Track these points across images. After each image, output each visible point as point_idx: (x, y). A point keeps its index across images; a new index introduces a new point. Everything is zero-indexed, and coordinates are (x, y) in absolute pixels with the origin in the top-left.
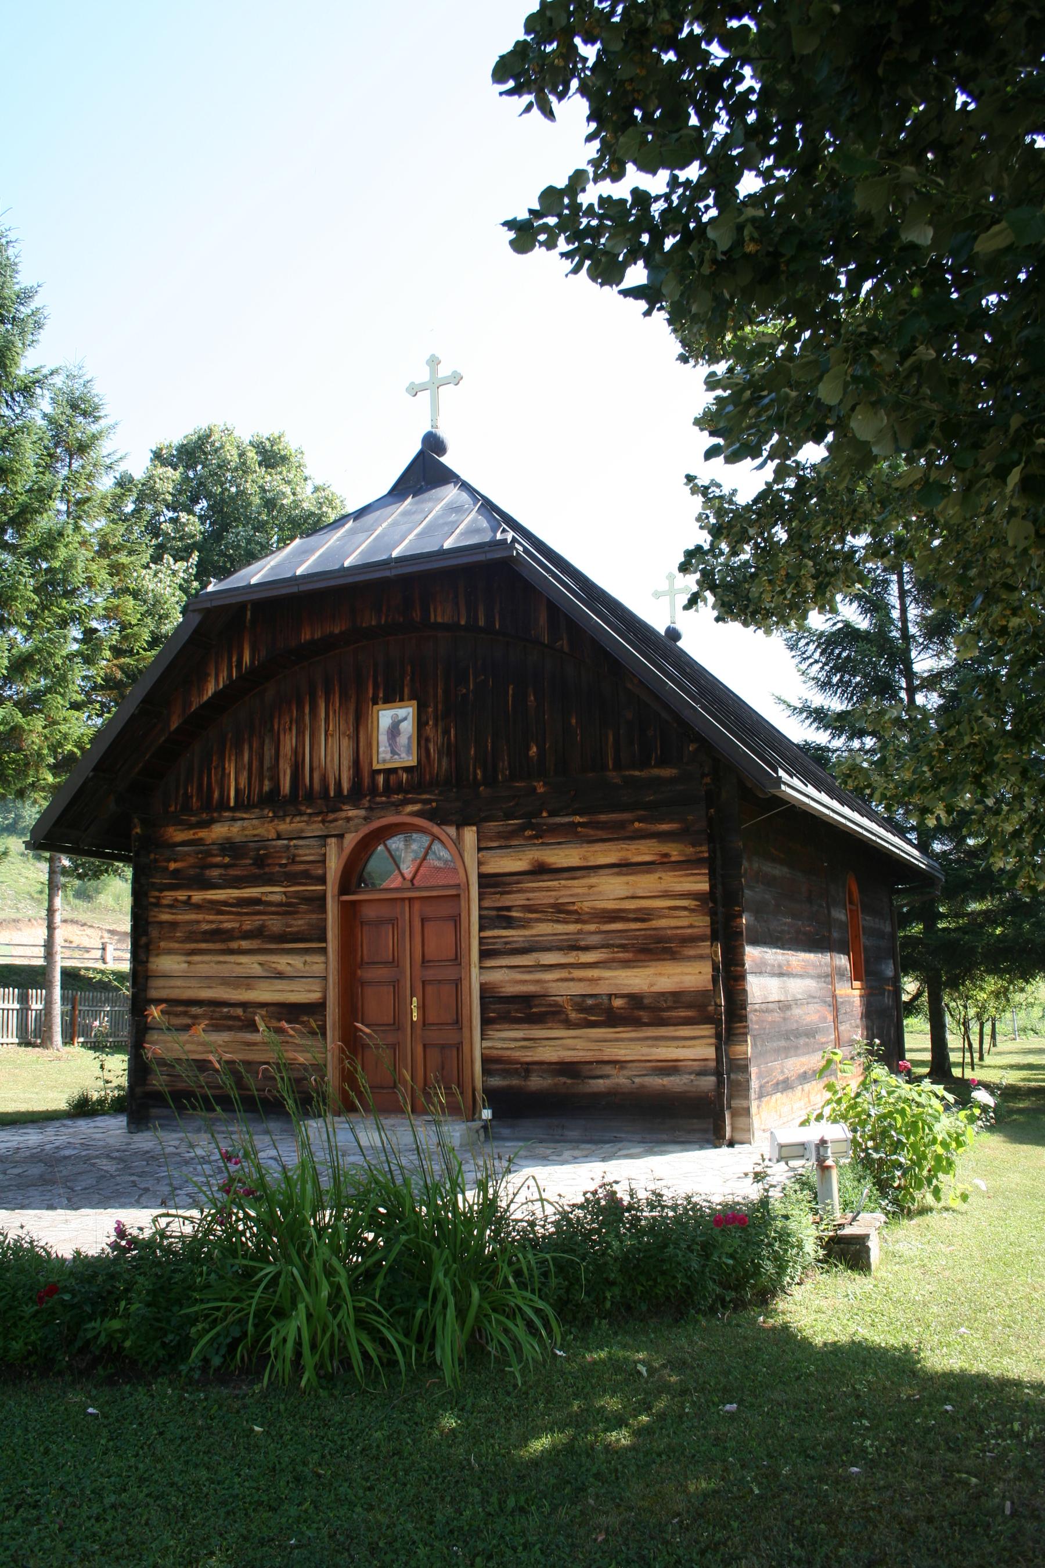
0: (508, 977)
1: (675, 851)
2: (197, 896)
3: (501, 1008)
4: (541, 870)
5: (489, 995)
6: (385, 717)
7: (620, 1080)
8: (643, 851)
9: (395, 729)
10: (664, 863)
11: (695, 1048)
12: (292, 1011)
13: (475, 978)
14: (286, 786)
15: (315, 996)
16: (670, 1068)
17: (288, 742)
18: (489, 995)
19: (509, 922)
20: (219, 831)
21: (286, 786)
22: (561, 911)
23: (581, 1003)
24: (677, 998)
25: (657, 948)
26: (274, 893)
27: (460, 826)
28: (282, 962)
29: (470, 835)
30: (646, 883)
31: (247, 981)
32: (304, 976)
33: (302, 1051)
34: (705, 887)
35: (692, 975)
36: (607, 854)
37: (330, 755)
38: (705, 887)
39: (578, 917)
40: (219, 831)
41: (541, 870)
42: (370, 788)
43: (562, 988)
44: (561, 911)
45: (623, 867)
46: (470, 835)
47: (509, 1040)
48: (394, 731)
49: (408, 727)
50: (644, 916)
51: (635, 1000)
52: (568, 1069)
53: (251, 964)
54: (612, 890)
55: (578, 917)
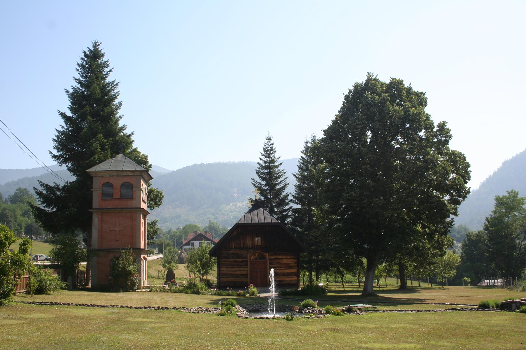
1: (292, 257)
2: (228, 260)
4: (276, 258)
6: (256, 239)
7: (286, 282)
8: (289, 257)
10: (291, 258)
11: (295, 278)
14: (242, 246)
15: (246, 273)
16: (292, 281)
17: (242, 241)
19: (273, 264)
20: (231, 252)
21: (242, 246)
22: (279, 263)
23: (281, 273)
24: (293, 273)
25: (290, 268)
26: (240, 260)
27: (266, 252)
28: (241, 269)
29: (267, 254)
30: (289, 260)
31: (236, 271)
32: (244, 271)
34: (296, 261)
35: (294, 271)
36: (285, 257)
37: (249, 243)
38: (296, 261)
39: (281, 264)
40: (231, 252)
41: (276, 258)
42: (254, 248)
44: (279, 263)
45: (286, 258)
46: (267, 254)
48: (258, 241)
49: (260, 240)
50: (289, 264)
51: (288, 273)
53: (237, 269)
54: (285, 261)
55: (281, 264)
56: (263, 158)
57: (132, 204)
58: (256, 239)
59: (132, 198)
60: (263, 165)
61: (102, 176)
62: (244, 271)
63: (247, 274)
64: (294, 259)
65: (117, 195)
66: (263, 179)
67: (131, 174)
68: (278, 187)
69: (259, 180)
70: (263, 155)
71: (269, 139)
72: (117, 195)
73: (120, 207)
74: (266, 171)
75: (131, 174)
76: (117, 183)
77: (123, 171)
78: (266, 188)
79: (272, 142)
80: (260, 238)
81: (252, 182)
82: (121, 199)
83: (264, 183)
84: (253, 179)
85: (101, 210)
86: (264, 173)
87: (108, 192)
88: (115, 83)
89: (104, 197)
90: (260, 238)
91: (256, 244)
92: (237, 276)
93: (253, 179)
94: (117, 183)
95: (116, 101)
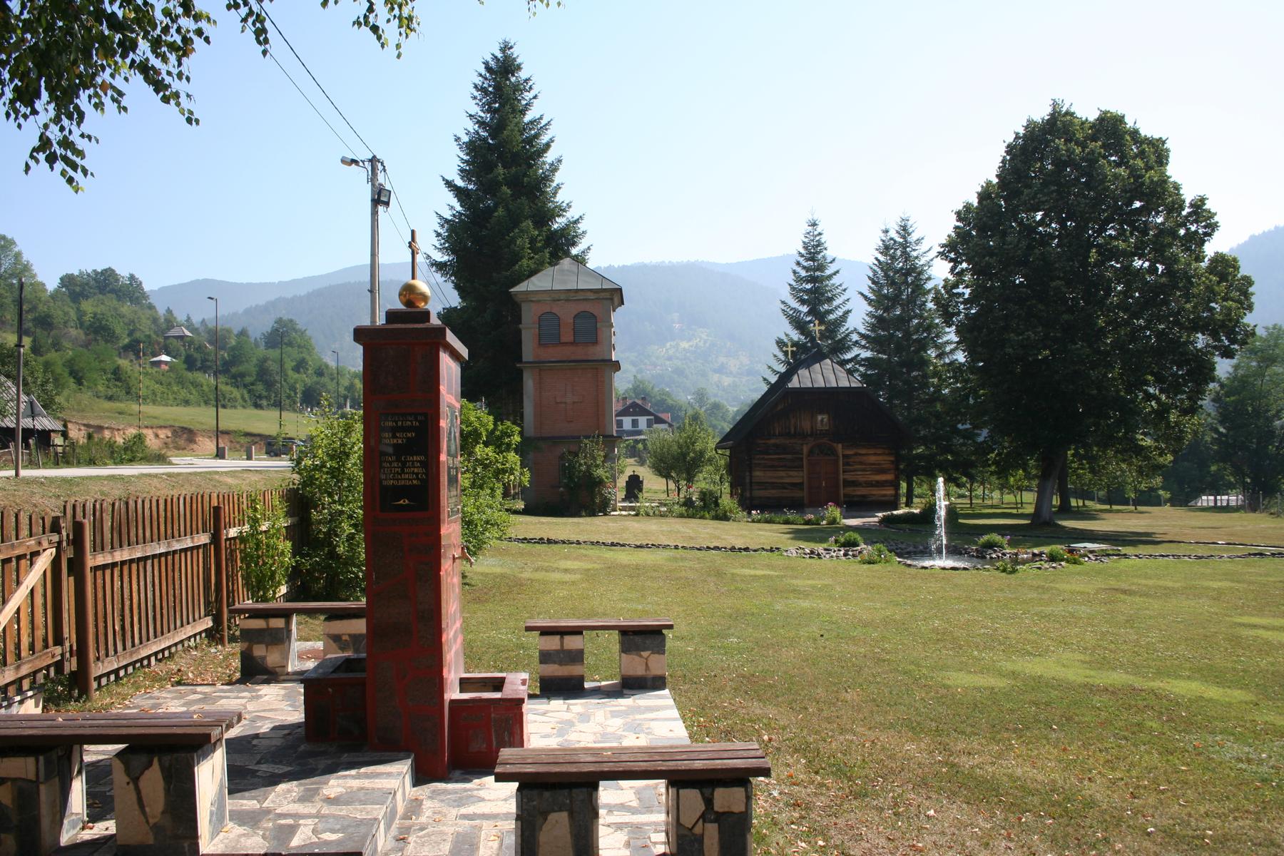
0: (849, 477)
3: (848, 483)
5: (844, 481)
6: (820, 418)
8: (879, 451)
9: (822, 419)
11: (890, 492)
12: (794, 485)
13: (841, 477)
16: (885, 495)
18: (844, 481)
20: (772, 441)
22: (861, 463)
25: (883, 471)
26: (789, 456)
28: (791, 473)
30: (881, 458)
31: (782, 477)
32: (796, 477)
33: (797, 494)
35: (890, 477)
36: (872, 451)
37: (806, 425)
40: (772, 441)
43: (861, 479)
44: (861, 463)
47: (849, 490)
51: (877, 482)
52: (863, 496)
53: (782, 474)
54: (873, 459)
56: (801, 260)
57: (596, 352)
58: (820, 418)
59: (595, 342)
60: (803, 273)
61: (539, 301)
62: (796, 477)
63: (802, 484)
64: (889, 454)
65: (567, 336)
66: (803, 302)
67: (592, 296)
68: (832, 317)
69: (795, 304)
70: (802, 256)
71: (814, 225)
72: (567, 336)
73: (573, 358)
74: (809, 286)
75: (592, 296)
76: (566, 313)
77: (577, 291)
78: (809, 319)
79: (819, 230)
80: (825, 417)
81: (783, 306)
82: (573, 343)
83: (805, 309)
84: (783, 302)
85: (538, 364)
86: (806, 291)
87: (549, 331)
88: (543, 122)
89: (542, 342)
90: (825, 417)
91: (819, 426)
92: (783, 486)
93: (783, 302)
94: (566, 313)
95: (549, 157)
